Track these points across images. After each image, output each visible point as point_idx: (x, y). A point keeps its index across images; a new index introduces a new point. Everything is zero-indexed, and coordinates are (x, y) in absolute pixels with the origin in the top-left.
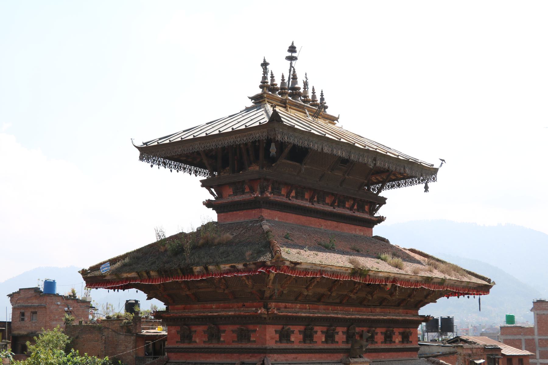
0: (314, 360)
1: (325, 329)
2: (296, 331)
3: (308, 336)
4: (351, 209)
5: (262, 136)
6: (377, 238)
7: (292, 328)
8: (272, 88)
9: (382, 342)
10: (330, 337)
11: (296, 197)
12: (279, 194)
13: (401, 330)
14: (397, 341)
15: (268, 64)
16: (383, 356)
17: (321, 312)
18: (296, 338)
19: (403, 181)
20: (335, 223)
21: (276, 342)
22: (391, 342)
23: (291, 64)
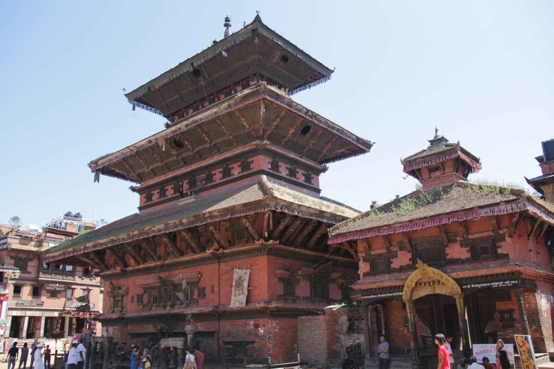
1: (172, 186)
2: (156, 193)
3: (163, 193)
9: (220, 179)
17: (170, 175)
18: (155, 198)
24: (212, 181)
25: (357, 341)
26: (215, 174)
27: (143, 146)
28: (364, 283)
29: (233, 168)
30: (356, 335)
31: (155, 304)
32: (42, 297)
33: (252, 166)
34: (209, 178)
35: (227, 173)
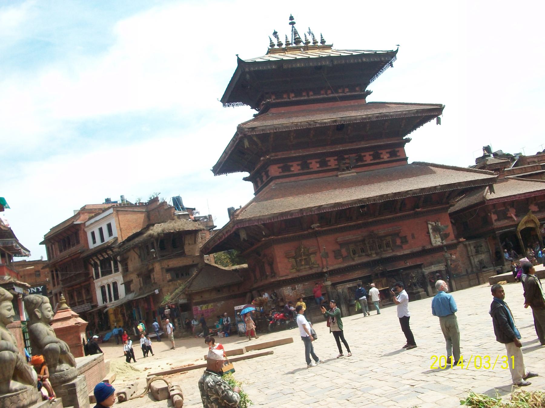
0: (312, 178)
3: (305, 165)
4: (343, 92)
5: (240, 72)
6: (369, 103)
7: (290, 164)
8: (280, 44)
9: (371, 160)
10: (323, 163)
11: (296, 97)
12: (283, 98)
13: (388, 150)
14: (385, 157)
15: (276, 33)
16: (372, 168)
17: (312, 151)
18: (295, 168)
19: (386, 66)
20: (331, 103)
21: (280, 173)
22: (379, 158)
23: (293, 27)
24: (362, 161)
25: (481, 258)
26: (365, 156)
27: (325, 123)
28: (497, 224)
29: (382, 153)
30: (480, 255)
31: (357, 255)
32: (169, 274)
33: (398, 154)
34: (360, 159)
35: (376, 156)
